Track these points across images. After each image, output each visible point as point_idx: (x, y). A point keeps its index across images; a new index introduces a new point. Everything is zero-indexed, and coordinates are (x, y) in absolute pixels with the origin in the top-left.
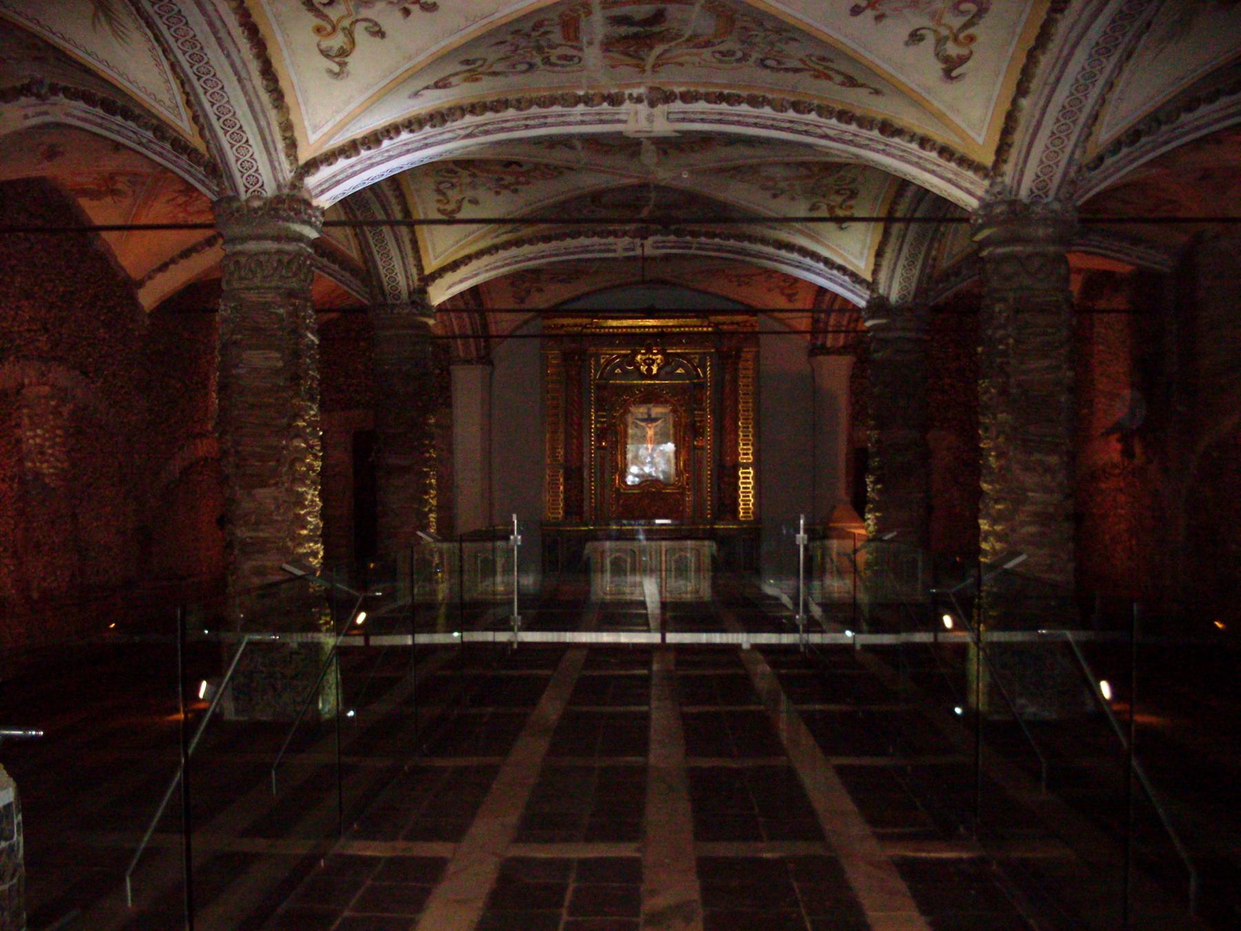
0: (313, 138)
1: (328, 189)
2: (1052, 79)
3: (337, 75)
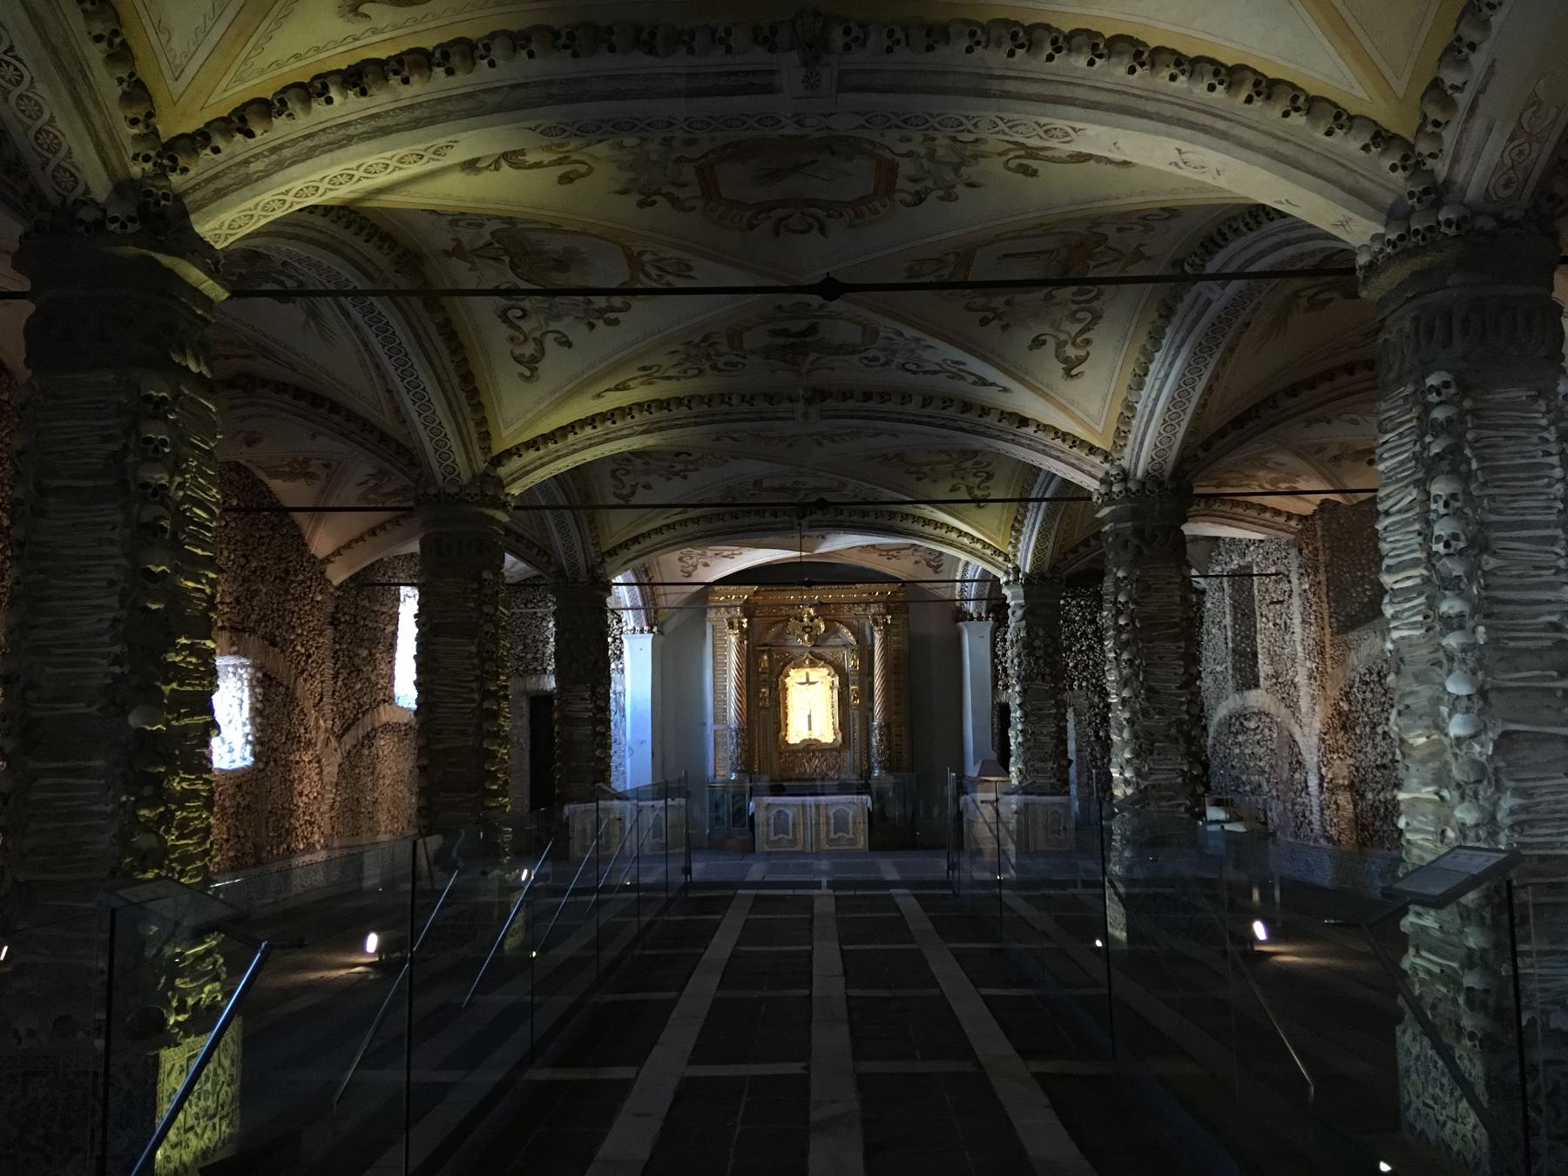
0: (505, 433)
1: (519, 478)
2: (1162, 374)
3: (528, 379)
